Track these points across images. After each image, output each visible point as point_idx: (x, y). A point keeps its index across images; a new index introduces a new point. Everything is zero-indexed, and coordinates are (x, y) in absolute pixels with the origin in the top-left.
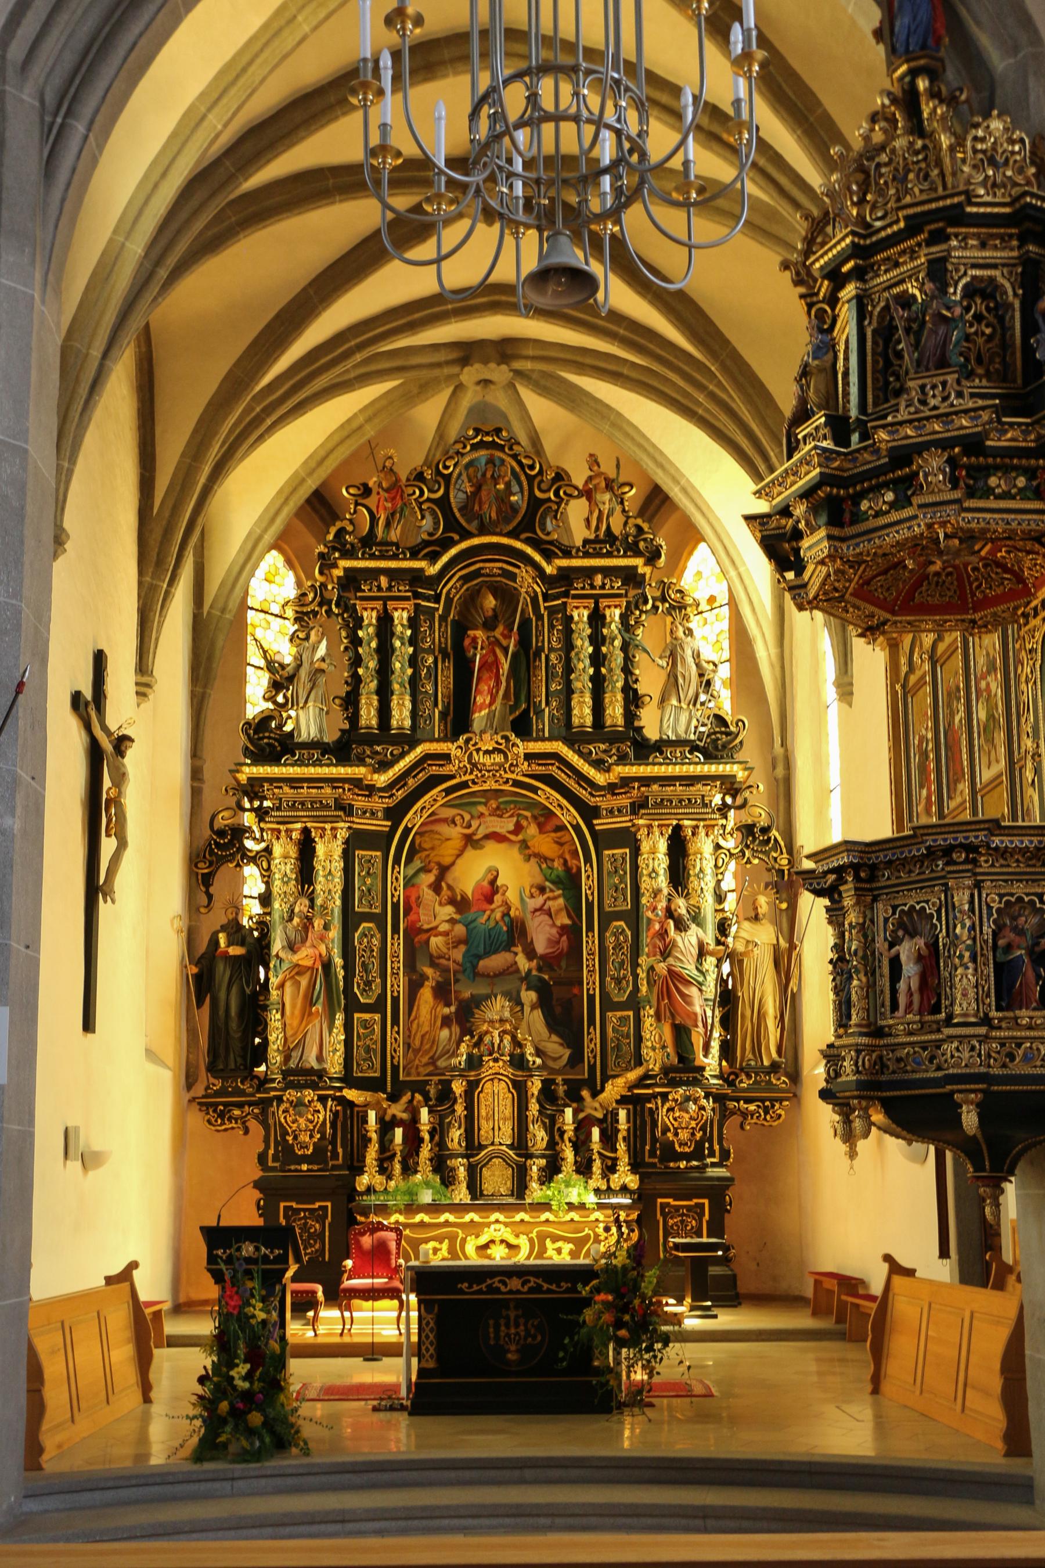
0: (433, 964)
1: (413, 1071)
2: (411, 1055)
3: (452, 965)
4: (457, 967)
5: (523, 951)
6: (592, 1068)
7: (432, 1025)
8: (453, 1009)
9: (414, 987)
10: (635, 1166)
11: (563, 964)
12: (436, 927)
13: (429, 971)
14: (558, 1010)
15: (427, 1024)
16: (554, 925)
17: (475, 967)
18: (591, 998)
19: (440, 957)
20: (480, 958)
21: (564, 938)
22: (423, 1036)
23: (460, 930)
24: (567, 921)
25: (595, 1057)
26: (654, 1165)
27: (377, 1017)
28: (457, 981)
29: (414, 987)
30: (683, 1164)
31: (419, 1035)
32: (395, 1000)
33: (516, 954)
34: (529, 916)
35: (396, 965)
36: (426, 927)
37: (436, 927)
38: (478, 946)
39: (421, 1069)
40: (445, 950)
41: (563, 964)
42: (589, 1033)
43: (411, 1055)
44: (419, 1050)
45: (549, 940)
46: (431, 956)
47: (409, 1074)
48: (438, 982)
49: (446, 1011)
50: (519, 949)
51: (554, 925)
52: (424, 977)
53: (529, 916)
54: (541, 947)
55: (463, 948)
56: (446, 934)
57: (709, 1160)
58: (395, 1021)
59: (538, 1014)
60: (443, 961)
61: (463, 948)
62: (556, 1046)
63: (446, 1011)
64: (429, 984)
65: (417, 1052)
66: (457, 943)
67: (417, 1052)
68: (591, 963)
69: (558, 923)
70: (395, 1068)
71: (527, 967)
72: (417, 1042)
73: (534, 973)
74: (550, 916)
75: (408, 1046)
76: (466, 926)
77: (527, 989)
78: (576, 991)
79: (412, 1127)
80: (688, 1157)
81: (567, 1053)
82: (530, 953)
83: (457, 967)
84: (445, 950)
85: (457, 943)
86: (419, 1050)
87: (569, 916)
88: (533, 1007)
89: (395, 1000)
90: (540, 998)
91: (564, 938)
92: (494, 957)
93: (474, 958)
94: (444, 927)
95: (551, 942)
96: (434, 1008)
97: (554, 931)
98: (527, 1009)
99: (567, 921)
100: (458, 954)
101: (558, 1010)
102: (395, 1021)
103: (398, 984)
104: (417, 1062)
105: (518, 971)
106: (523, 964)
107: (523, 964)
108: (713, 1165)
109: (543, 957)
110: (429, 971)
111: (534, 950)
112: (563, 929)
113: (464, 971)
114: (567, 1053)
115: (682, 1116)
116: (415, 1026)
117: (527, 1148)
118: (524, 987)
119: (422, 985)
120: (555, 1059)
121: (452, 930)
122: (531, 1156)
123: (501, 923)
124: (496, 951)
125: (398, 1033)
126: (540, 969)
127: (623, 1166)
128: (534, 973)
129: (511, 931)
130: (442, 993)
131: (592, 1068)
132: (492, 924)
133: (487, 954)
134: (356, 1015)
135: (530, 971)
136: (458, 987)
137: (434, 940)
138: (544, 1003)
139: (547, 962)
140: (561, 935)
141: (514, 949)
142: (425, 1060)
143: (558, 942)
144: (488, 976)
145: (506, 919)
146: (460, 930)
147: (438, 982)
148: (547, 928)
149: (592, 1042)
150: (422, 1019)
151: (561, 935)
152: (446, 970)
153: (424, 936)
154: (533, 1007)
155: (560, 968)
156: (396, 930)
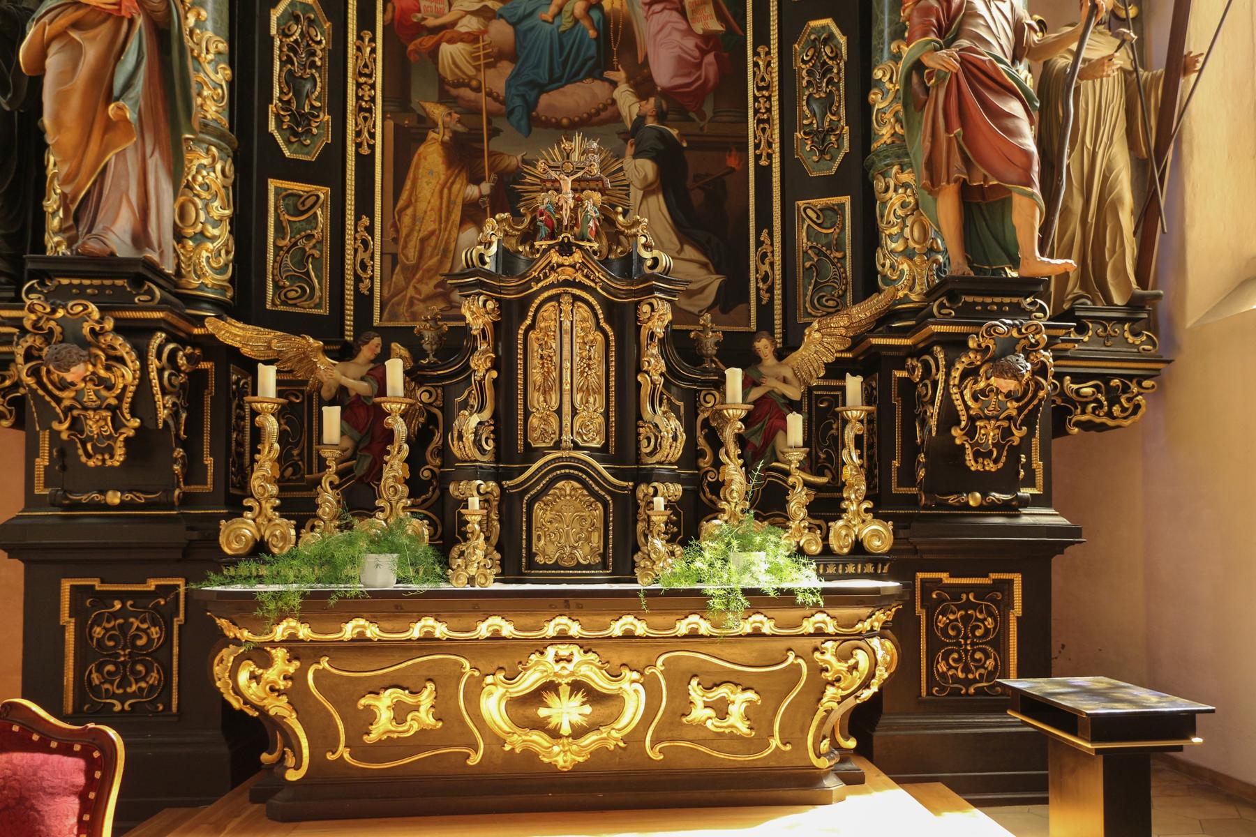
0: (445, 98)
1: (403, 309)
2: (398, 278)
3: (484, 101)
4: (495, 106)
5: (628, 81)
6: (765, 311)
7: (443, 219)
8: (486, 188)
9: (406, 142)
10: (881, 502)
11: (708, 109)
12: (453, 24)
13: (438, 112)
14: (697, 197)
15: (433, 216)
16: (690, 32)
17: (531, 106)
18: (764, 174)
19: (459, 84)
20: (543, 89)
21: (710, 58)
22: (423, 241)
23: (501, 31)
24: (715, 26)
25: (770, 290)
26: (912, 501)
27: (323, 192)
28: (494, 133)
29: (406, 142)
30: (975, 499)
31: (414, 243)
32: (365, 163)
33: (614, 84)
34: (640, 11)
35: (367, 93)
36: (431, 22)
37: (453, 24)
38: (537, 66)
39: (419, 307)
40: (471, 71)
41: (708, 109)
42: (759, 243)
43: (398, 278)
44: (416, 268)
45: (681, 61)
46: (442, 80)
47: (394, 316)
48: (455, 133)
49: (473, 191)
50: (620, 75)
51: (690, 32)
52: (426, 123)
53: (640, 11)
54: (663, 73)
55: (506, 68)
56: (473, 38)
57: (1025, 492)
58: (364, 205)
59: (657, 203)
60: (466, 93)
61: (506, 68)
62: (693, 269)
63: (473, 191)
64: (436, 137)
65: (411, 271)
66: (494, 58)
67: (411, 271)
68: (762, 105)
69: (698, 28)
70: (364, 302)
71: (635, 110)
72: (412, 253)
73: (650, 123)
74: (682, 12)
75: (392, 259)
76: (514, 25)
77: (635, 156)
78: (732, 162)
79: (365, 417)
80: (984, 482)
81: (714, 282)
82: (643, 85)
83: (495, 106)
84: (471, 71)
85: (494, 58)
86: (416, 268)
87: (720, 17)
88: (648, 191)
89: (365, 163)
90: (662, 173)
91: (710, 58)
92: (569, 88)
93: (529, 89)
94: (469, 25)
95: (685, 65)
96: (446, 185)
97: (690, 43)
98: (636, 194)
99: (715, 26)
100: (498, 79)
101: (697, 197)
102: (364, 205)
103: (372, 130)
104: (411, 292)
105: (617, 117)
106: (628, 104)
107: (628, 104)
108: (1035, 501)
109: (667, 93)
110: (438, 112)
111: (649, 79)
112: (708, 37)
113: (511, 112)
114: (714, 282)
115: (978, 396)
116: (407, 220)
117: (638, 461)
118: (630, 150)
119: (422, 139)
120: (690, 294)
121: (485, 32)
122: (647, 476)
123: (585, 23)
124: (574, 78)
125: (370, 230)
126: (661, 116)
127: (855, 500)
128: (650, 123)
129: (604, 39)
130: (464, 154)
131: (765, 311)
132: (565, 23)
133: (556, 81)
134: (273, 184)
135: (641, 118)
136: (496, 145)
137: (446, 50)
138: (670, 183)
139: (676, 103)
140: (704, 53)
141: (609, 74)
142: (428, 288)
143: (698, 66)
144: (558, 125)
145: (595, 15)
146: (501, 31)
147: (455, 133)
148: (677, 36)
149: (764, 263)
150: (422, 206)
151: (704, 53)
152: (475, 111)
153: (427, 41)
154: (648, 191)
155: (702, 116)
156: (366, 21)
